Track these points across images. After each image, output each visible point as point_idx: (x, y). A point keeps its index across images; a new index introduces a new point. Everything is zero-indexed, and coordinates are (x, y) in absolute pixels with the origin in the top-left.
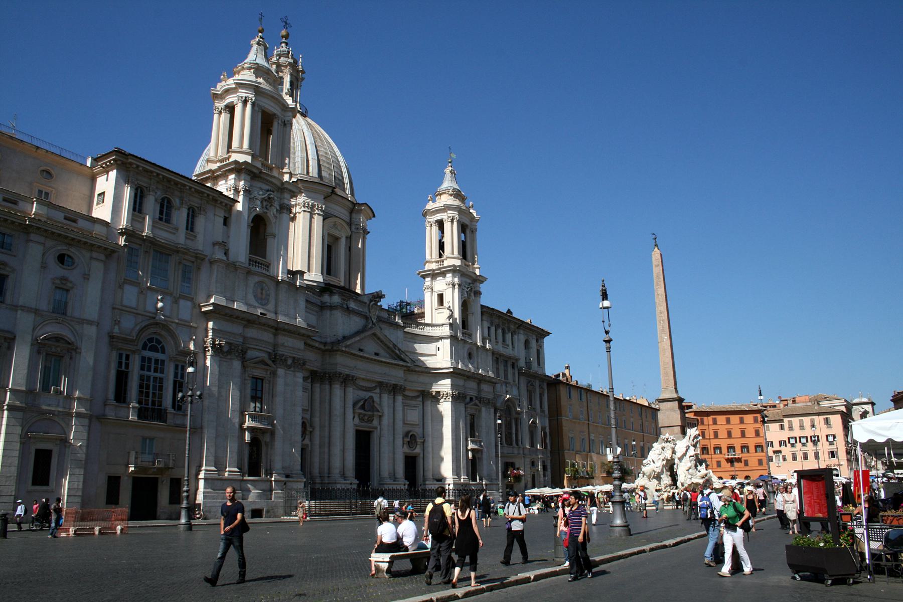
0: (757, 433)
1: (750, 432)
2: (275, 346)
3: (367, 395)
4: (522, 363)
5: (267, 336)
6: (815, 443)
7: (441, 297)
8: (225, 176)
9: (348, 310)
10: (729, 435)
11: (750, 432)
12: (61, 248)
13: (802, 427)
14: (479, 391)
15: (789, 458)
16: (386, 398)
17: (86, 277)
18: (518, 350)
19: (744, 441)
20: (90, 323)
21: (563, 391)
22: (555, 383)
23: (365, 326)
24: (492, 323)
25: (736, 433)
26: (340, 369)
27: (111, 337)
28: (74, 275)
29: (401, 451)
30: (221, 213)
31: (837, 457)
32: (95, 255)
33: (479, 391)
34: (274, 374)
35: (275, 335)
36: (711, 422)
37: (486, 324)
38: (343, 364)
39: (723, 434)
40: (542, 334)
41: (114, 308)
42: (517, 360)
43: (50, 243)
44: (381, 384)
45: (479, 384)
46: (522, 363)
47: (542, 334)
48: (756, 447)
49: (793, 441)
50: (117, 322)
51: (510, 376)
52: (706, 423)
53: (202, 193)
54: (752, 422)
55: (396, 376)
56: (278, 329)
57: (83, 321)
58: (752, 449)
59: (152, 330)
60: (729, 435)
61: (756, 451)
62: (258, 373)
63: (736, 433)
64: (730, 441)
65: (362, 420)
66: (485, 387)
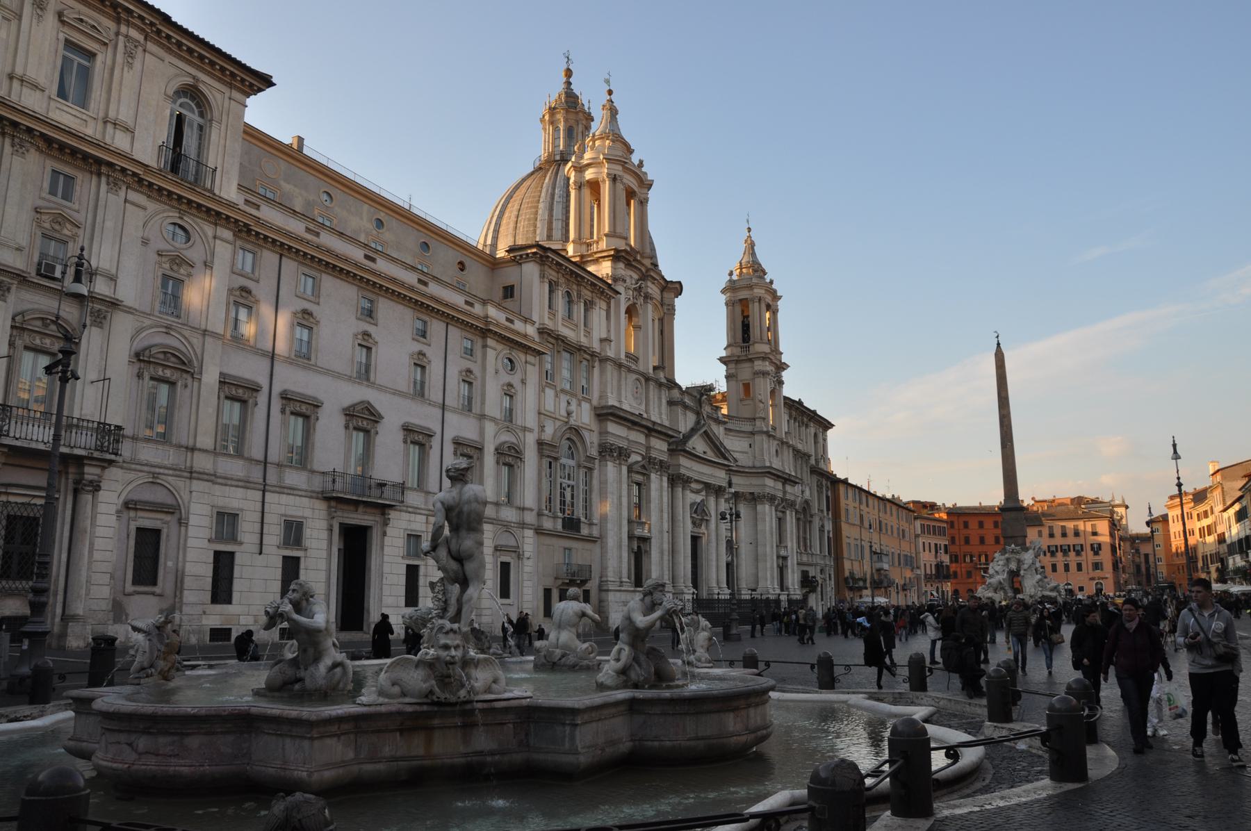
2: (648, 448)
3: (698, 498)
4: (813, 461)
5: (638, 437)
6: (1078, 553)
7: (747, 387)
8: (596, 261)
9: (686, 407)
10: (982, 540)
12: (505, 351)
13: (1064, 535)
14: (785, 492)
16: (712, 500)
17: (523, 382)
18: (807, 447)
20: (531, 430)
21: (842, 488)
22: (835, 482)
23: (698, 423)
24: (790, 416)
26: (682, 471)
27: (540, 444)
28: (515, 380)
29: (724, 559)
30: (604, 305)
32: (530, 358)
33: (785, 492)
34: (648, 477)
35: (647, 436)
36: (962, 526)
37: (786, 417)
38: (687, 466)
39: (975, 540)
40: (827, 425)
41: (540, 413)
42: (809, 456)
43: (500, 347)
44: (707, 486)
45: (784, 484)
46: (813, 461)
47: (827, 425)
50: (542, 428)
51: (805, 475)
53: (595, 285)
55: (719, 477)
56: (651, 430)
57: (525, 429)
59: (568, 436)
62: (639, 478)
65: (694, 523)
66: (788, 488)
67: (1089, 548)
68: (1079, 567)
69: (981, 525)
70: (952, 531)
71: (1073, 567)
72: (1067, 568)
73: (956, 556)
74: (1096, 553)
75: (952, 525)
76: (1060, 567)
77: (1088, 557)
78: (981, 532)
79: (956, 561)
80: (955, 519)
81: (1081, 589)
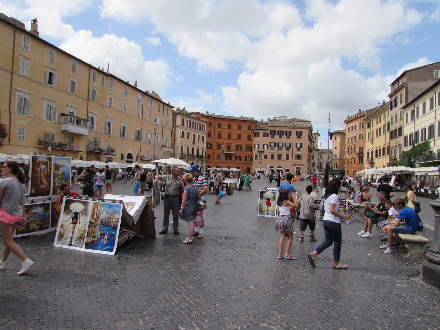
0: (249, 138)
1: (244, 137)
6: (288, 149)
11: (244, 137)
15: (269, 157)
19: (239, 142)
25: (234, 136)
31: (301, 159)
36: (217, 126)
39: (224, 136)
48: (247, 147)
49: (273, 145)
52: (213, 126)
54: (246, 129)
58: (244, 148)
60: (229, 136)
61: (246, 150)
63: (234, 136)
64: (229, 141)
67: (295, 145)
68: (288, 157)
69: (230, 127)
70: (210, 129)
71: (284, 157)
72: (280, 157)
73: (211, 145)
74: (299, 149)
75: (210, 125)
76: (276, 157)
77: (294, 151)
78: (229, 131)
79: (211, 148)
80: (213, 121)
81: (287, 170)
